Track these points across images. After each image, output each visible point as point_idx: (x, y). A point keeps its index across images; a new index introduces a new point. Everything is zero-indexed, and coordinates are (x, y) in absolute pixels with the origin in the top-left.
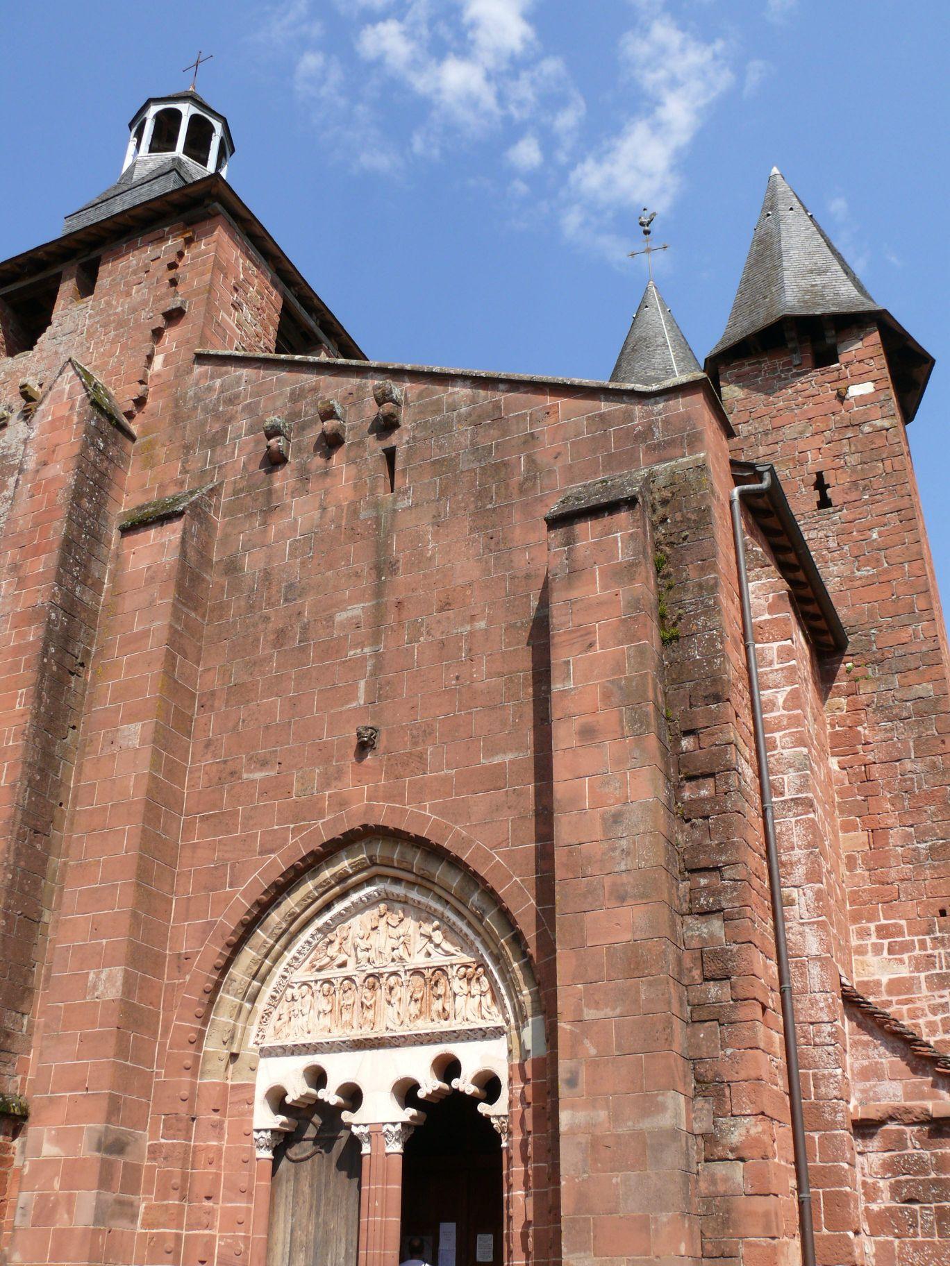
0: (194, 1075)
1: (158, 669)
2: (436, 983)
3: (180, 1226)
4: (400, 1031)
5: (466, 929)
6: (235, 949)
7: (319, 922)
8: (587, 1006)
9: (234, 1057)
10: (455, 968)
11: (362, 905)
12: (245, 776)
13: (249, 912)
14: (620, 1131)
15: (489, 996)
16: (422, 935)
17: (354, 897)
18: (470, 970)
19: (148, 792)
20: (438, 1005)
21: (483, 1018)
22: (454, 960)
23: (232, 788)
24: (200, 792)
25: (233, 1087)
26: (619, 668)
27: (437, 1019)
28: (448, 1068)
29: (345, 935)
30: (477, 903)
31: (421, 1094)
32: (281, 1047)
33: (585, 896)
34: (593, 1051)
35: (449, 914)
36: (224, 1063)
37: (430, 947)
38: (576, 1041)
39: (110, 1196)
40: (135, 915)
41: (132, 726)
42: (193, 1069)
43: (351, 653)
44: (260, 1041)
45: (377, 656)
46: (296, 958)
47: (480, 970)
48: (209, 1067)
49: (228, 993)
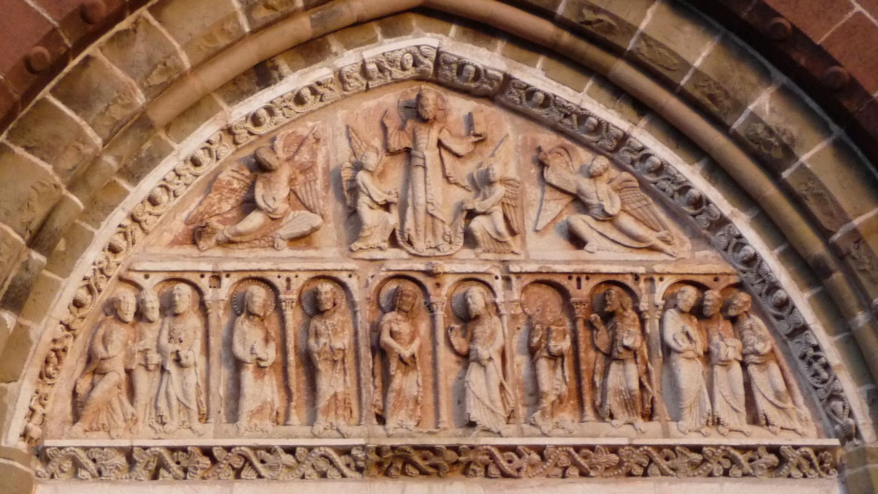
2: (608, 317)
5: (700, 184)
7: (238, 113)
10: (661, 288)
13: (51, 38)
15: (774, 369)
17: (347, 59)
22: (658, 262)
29: (304, 156)
32: (120, 449)
35: (644, 137)
37: (582, 223)
44: (36, 431)
46: (153, 201)
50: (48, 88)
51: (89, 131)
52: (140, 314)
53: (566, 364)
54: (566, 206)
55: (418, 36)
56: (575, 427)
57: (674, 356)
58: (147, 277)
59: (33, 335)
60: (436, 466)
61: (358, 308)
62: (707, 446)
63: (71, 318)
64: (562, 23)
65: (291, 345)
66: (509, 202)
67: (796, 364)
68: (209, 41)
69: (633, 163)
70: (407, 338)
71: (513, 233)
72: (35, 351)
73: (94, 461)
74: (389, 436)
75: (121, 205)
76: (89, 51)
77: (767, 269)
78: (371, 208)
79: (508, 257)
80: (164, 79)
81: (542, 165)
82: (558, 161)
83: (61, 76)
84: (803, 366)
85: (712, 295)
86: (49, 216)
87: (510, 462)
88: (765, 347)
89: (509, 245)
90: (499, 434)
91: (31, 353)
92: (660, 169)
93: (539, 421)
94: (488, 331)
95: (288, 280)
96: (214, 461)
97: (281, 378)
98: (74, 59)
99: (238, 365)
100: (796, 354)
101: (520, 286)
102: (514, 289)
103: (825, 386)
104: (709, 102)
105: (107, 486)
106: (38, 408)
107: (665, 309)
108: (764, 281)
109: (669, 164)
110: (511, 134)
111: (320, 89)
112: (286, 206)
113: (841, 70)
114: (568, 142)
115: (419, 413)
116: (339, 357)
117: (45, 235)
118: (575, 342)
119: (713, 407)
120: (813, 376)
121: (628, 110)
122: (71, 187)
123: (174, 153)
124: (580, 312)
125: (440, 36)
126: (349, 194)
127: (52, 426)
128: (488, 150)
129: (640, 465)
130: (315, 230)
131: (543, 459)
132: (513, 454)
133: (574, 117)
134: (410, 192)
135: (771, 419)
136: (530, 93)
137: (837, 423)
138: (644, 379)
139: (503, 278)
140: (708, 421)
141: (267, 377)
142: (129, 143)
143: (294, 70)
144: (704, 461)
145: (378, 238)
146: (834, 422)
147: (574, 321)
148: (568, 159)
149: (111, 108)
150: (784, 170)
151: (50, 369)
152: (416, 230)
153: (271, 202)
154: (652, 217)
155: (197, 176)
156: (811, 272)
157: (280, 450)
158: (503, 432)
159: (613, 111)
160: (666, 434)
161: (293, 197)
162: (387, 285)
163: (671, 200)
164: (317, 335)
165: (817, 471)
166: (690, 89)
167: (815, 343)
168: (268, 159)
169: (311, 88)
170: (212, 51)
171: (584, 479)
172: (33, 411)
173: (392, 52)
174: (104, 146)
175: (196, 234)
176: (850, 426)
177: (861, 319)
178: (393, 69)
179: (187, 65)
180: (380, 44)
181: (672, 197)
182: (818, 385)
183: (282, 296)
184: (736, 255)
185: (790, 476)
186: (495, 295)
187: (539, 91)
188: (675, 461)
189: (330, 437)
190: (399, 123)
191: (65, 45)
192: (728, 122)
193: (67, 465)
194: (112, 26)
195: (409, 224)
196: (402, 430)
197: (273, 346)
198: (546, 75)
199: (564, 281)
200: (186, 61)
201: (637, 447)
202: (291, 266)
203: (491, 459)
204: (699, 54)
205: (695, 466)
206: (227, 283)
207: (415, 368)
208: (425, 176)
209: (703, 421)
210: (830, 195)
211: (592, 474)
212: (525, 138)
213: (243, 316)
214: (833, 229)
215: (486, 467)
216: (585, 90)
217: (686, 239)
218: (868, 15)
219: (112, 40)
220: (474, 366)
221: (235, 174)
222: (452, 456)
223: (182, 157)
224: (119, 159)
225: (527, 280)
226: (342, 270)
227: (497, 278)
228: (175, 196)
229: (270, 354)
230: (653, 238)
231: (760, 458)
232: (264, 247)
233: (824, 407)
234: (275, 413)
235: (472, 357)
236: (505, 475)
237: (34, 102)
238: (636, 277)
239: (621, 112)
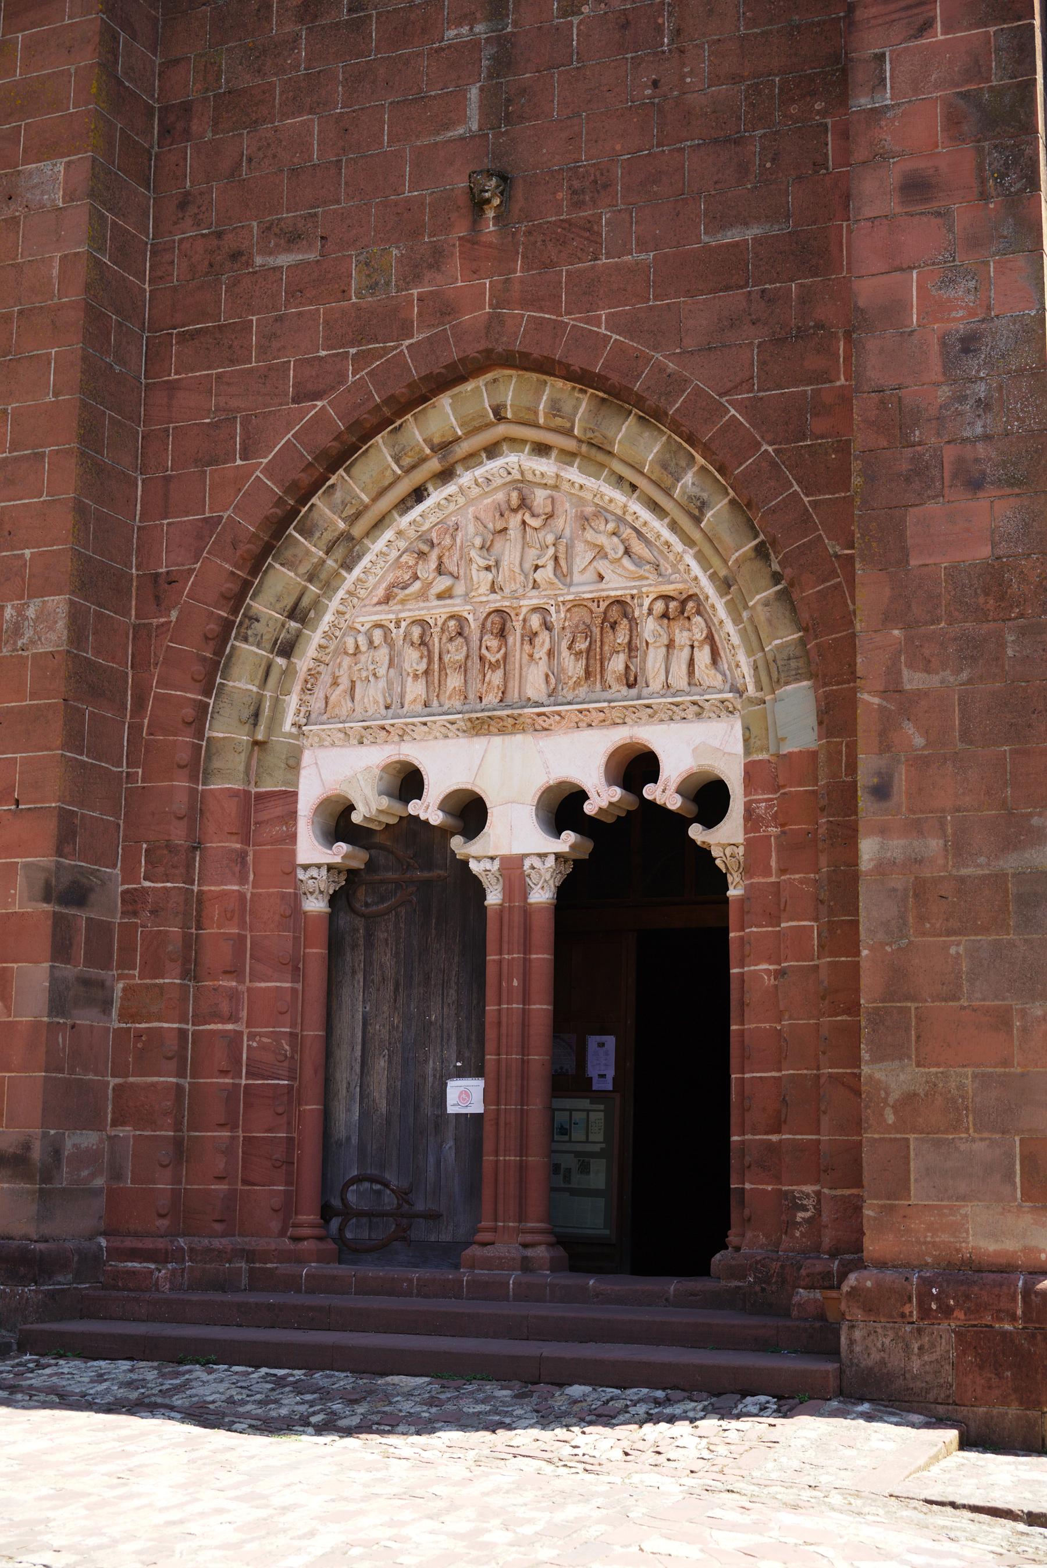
0: (194, 778)
1: (88, 58)
3: (183, 1019)
5: (667, 534)
6: (257, 564)
7: (404, 521)
8: (910, 666)
9: (256, 743)
10: (647, 602)
11: (476, 491)
12: (259, 260)
13: (280, 502)
14: (964, 872)
15: (707, 649)
16: (587, 542)
17: (465, 478)
18: (673, 605)
19: (88, 287)
20: (617, 664)
23: (236, 282)
24: (175, 289)
25: (260, 796)
26: (976, 70)
27: (615, 687)
28: (637, 767)
31: (589, 808)
32: (340, 730)
33: (907, 480)
34: (919, 741)
36: (243, 756)
37: (602, 566)
38: (887, 725)
39: (68, 971)
40: (80, 509)
41: (45, 166)
42: (197, 766)
43: (452, 33)
45: (502, 42)
46: (359, 580)
47: (691, 604)
48: (217, 764)
49: (246, 640)
50: (292, 527)
55: (507, 456)
59: (298, 668)
74: (483, 710)
76: (314, 500)
79: (557, 592)
90: (542, 705)
112: (435, 574)
115: (500, 694)
117: (298, 611)
122: (310, 580)
127: (313, 716)
131: (563, 718)
144: (655, 712)
145: (484, 588)
151: (309, 686)
156: (725, 585)
164: (448, 652)
166: (649, 475)
177: (745, 615)
193: (317, 739)
197: (425, 660)
199: (590, 604)
200: (366, 499)
202: (436, 612)
218: (738, 416)
219: (324, 492)
224: (336, 561)
238: (633, 597)
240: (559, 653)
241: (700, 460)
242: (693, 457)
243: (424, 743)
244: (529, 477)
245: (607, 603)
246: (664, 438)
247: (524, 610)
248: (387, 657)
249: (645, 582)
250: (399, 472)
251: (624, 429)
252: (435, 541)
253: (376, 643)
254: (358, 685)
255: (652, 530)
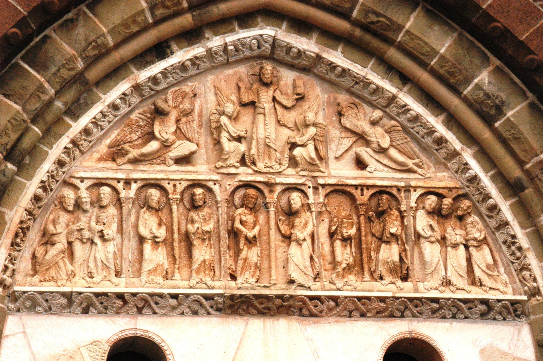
2: (381, 214)
4: (317, 290)
5: (441, 130)
7: (144, 75)
10: (414, 196)
13: (22, 23)
17: (216, 42)
21: (474, 281)
22: (414, 180)
27: (388, 278)
29: (186, 105)
30: (487, 87)
32: (63, 294)
35: (406, 98)
37: (365, 153)
46: (87, 132)
47: (466, 203)
50: (19, 55)
51: (46, 85)
52: (78, 205)
53: (353, 244)
54: (355, 142)
55: (261, 28)
56: (359, 285)
57: (422, 240)
58: (82, 181)
59: (7, 218)
60: (269, 309)
61: (219, 205)
62: (442, 299)
63: (33, 207)
64: (355, 23)
65: (175, 228)
66: (318, 138)
67: (500, 247)
68: (126, 29)
69: (398, 114)
70: (252, 225)
71: (321, 159)
72: (8, 229)
73: (47, 301)
74: (239, 288)
75: (66, 134)
77: (483, 185)
78: (229, 140)
80: (96, 52)
81: (340, 114)
82: (350, 112)
83: (28, 48)
84: (504, 248)
85: (447, 201)
86: (19, 139)
87: (316, 306)
88: (480, 235)
89: (319, 167)
91: (6, 230)
92: (416, 118)
93: (336, 281)
94: (304, 222)
95: (175, 186)
96: (125, 302)
97: (169, 249)
98: (36, 37)
99: (142, 240)
100: (501, 240)
101: (324, 194)
102: (321, 195)
103: (518, 261)
104: (448, 76)
105: (55, 317)
106: (10, 266)
107: (417, 209)
108: (481, 193)
109: (422, 116)
110: (320, 94)
111: (198, 62)
113: (536, 57)
114: (357, 100)
115: (258, 273)
116: (207, 236)
117: (17, 152)
118: (359, 230)
119: (446, 274)
120: (511, 255)
121: (396, 80)
122: (34, 121)
123: (101, 101)
124: (362, 210)
125: (276, 28)
126: (215, 131)
127: (19, 277)
128: (305, 105)
129: (399, 310)
130: (193, 153)
131: (337, 305)
132: (318, 301)
133: (362, 84)
134: (254, 130)
135: (484, 283)
136: (333, 67)
137: (526, 285)
138: (403, 255)
139: (313, 187)
140: (443, 283)
141: (160, 249)
142: (72, 94)
143: (181, 48)
145: (233, 160)
146: (524, 285)
147: (359, 217)
148: (357, 111)
149: (61, 70)
150: (496, 122)
151: (18, 240)
152: (258, 155)
153: (164, 135)
154: (410, 150)
155: (116, 116)
156: (512, 188)
157: (168, 296)
158: (312, 287)
159: (387, 81)
160: (416, 290)
161: (178, 131)
162: (239, 190)
163: (422, 139)
164: (193, 222)
165: (512, 316)
166: (437, 68)
167: (513, 233)
168: (162, 107)
169: (190, 60)
170: (127, 35)
171: (363, 318)
172: (6, 268)
173: (244, 38)
174: (56, 95)
175: (116, 153)
176: (535, 288)
178: (244, 50)
179: (111, 43)
180: (238, 33)
181: (423, 137)
182: (514, 261)
183: (170, 196)
184: (463, 176)
185: (495, 319)
186: (308, 198)
187: (339, 66)
188: (422, 308)
189: (201, 288)
190: (248, 85)
191: (31, 28)
192: (461, 90)
193: (28, 304)
194: (62, 16)
195: (253, 151)
196: (246, 285)
198: (344, 56)
199: (353, 191)
200: (111, 41)
201: (398, 298)
203: (303, 304)
204: (444, 45)
205: (434, 312)
206: (134, 186)
207: (256, 245)
208: (265, 120)
209: (440, 283)
210: (525, 138)
211: (368, 315)
212: (329, 97)
213: (145, 208)
214: (527, 161)
215: (301, 309)
216: (369, 67)
217: (431, 165)
219: (61, 25)
220: (293, 244)
221: (141, 116)
222: (278, 302)
223: (107, 103)
224: (65, 104)
225: (329, 189)
226: (209, 180)
227: (309, 187)
228: (102, 129)
229: (162, 233)
230: (410, 163)
231: (476, 307)
232: (159, 164)
233: (518, 275)
234: (165, 272)
235: (293, 239)
236: (312, 315)
237: (10, 65)
239: (391, 81)
240: (318, 239)
241: (497, 62)
242: (487, 58)
243: (165, 319)
244: (280, 54)
245: (371, 192)
246: (455, 35)
247: (279, 189)
248: (116, 220)
249: (412, 176)
250: (151, 21)
251: (412, 19)
252: (170, 103)
253: (105, 203)
254: (78, 247)
255: (424, 125)
